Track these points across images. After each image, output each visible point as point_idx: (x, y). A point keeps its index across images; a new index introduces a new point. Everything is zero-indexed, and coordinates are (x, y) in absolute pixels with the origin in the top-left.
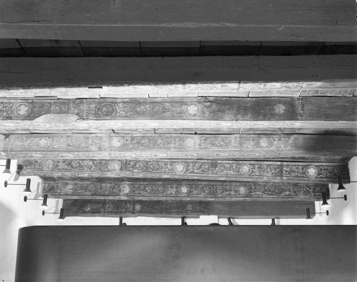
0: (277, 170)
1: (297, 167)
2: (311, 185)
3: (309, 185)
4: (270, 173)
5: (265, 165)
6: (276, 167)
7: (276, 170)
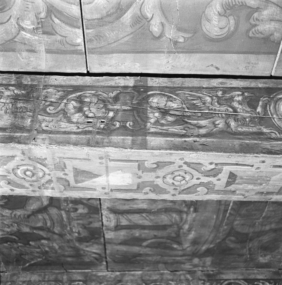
0: (117, 107)
1: (220, 93)
2: (259, 277)
3: (252, 277)
4: (76, 117)
5: (56, 86)
6: (112, 95)
7: (110, 107)
